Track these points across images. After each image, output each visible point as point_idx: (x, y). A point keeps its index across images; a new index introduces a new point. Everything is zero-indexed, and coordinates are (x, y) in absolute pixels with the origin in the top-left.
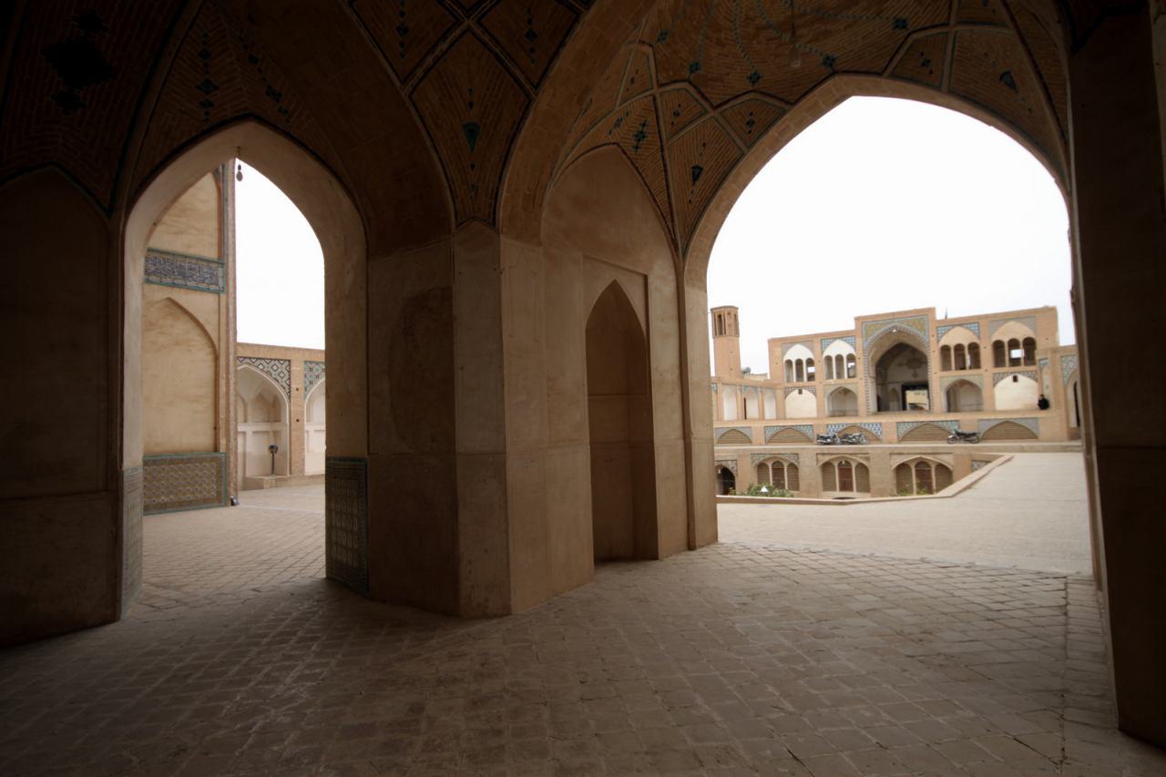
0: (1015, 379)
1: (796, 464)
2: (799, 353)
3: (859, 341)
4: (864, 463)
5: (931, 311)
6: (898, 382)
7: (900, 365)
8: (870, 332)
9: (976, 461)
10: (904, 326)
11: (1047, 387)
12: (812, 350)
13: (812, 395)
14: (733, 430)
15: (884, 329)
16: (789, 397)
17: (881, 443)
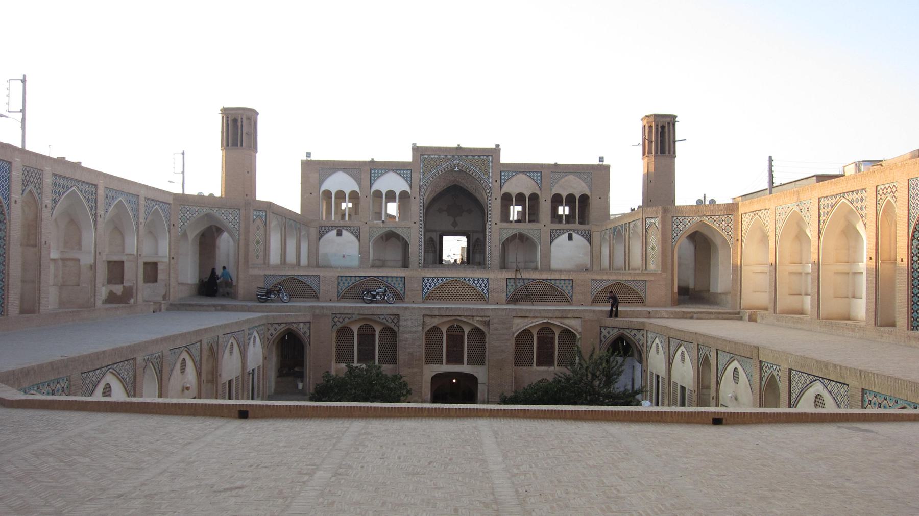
0: (570, 238)
1: (396, 329)
3: (416, 176)
4: (481, 327)
5: (496, 150)
6: (435, 231)
8: (429, 168)
9: (605, 327)
10: (467, 165)
11: (653, 248)
12: (359, 182)
13: (353, 238)
14: (293, 278)
15: (445, 165)
16: (322, 240)
17: (487, 303)
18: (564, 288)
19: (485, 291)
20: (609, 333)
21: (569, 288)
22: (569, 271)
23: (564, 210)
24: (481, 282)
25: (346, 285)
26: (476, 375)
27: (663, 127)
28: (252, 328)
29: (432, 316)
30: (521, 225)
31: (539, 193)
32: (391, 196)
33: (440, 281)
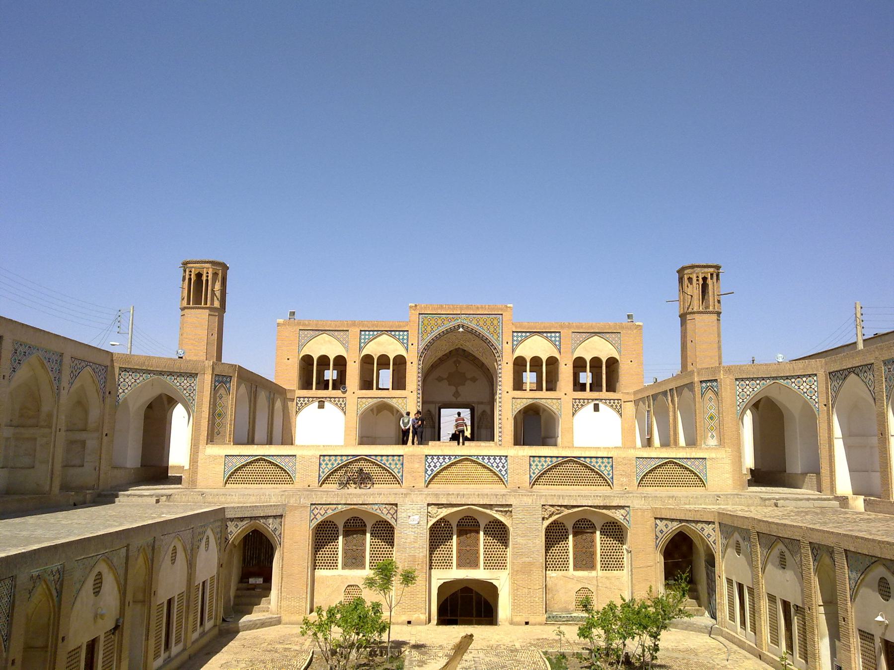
0: (596, 408)
1: (392, 522)
2: (325, 346)
3: (413, 339)
6: (432, 402)
7: (440, 379)
9: (661, 519)
10: (473, 325)
18: (603, 468)
19: (503, 473)
20: (666, 526)
21: (609, 468)
22: (607, 449)
23: (586, 378)
24: (498, 461)
25: (330, 466)
26: (495, 582)
27: (705, 279)
28: (204, 526)
29: (439, 505)
30: (538, 394)
31: (557, 356)
32: (384, 361)
33: (447, 460)
